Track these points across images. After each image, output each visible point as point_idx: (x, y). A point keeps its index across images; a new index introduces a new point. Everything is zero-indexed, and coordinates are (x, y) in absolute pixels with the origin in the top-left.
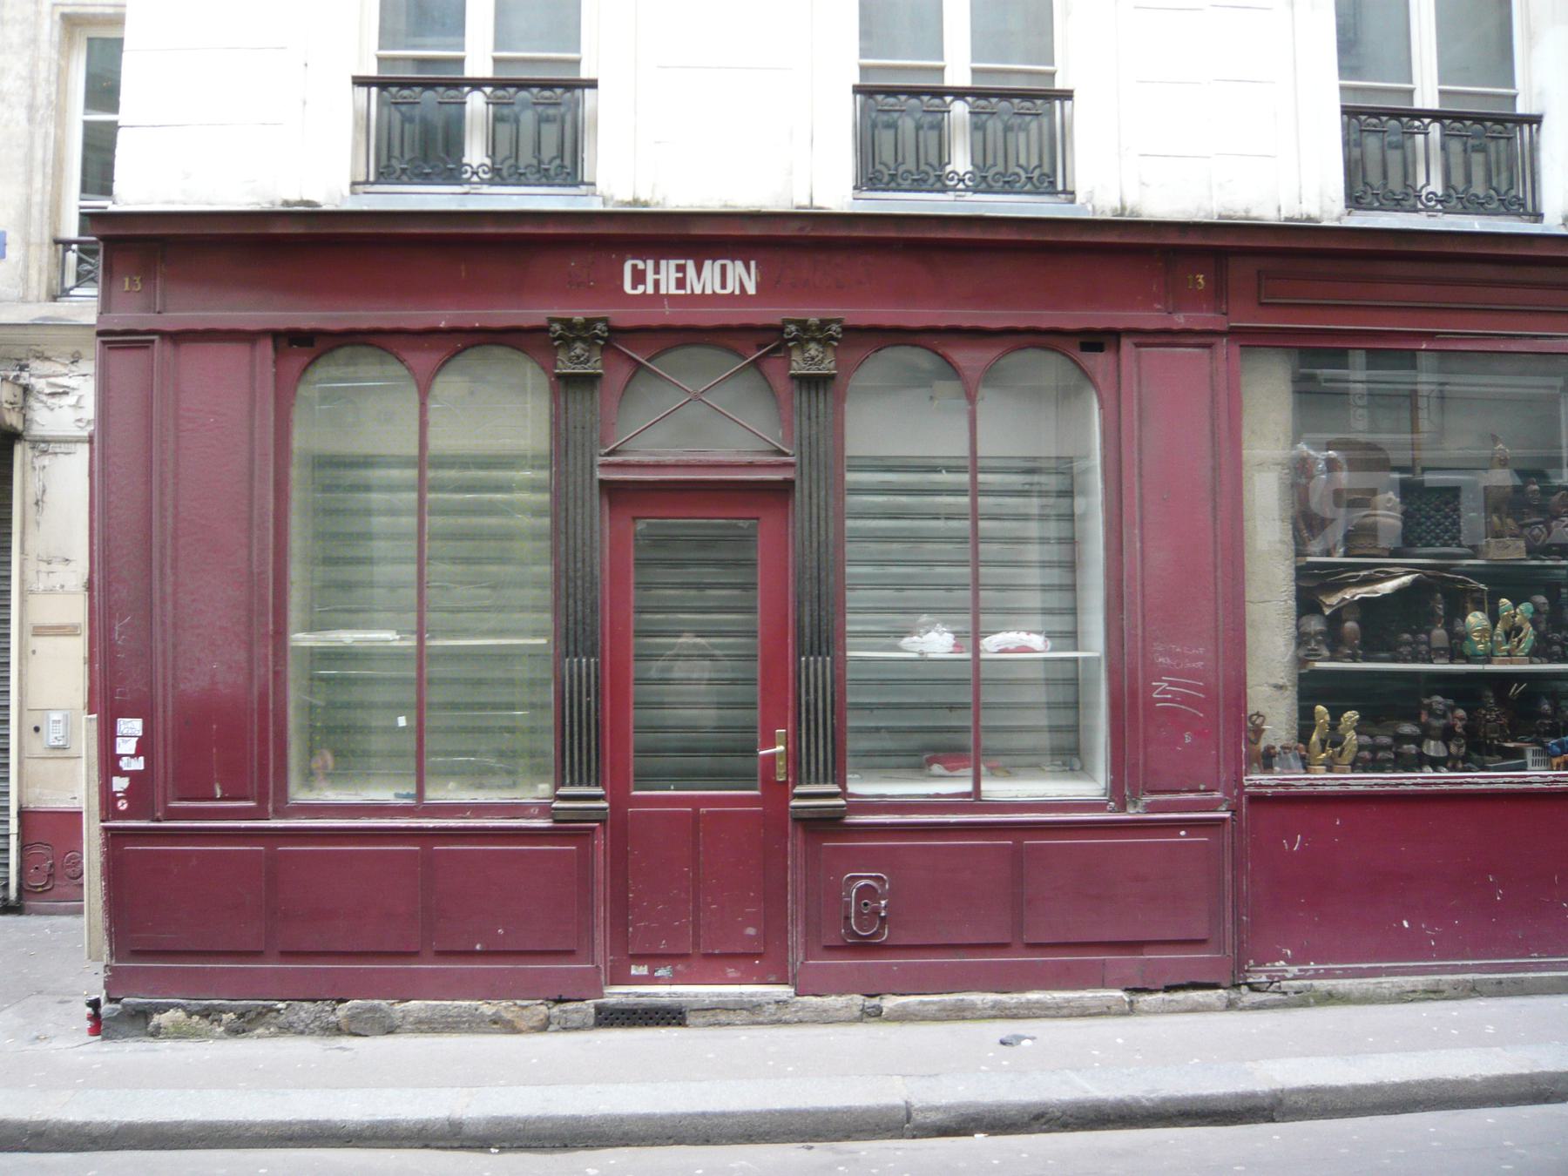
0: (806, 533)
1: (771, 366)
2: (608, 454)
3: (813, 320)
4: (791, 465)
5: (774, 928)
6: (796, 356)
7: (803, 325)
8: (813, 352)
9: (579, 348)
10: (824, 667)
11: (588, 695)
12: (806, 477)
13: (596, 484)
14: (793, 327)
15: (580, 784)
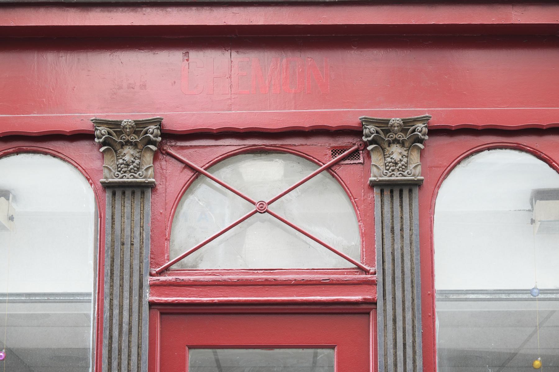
0: (390, 361)
1: (349, 171)
2: (160, 273)
3: (396, 121)
4: (373, 283)
6: (376, 159)
7: (384, 126)
8: (396, 157)
12: (389, 297)
13: (146, 307)
14: (372, 128)
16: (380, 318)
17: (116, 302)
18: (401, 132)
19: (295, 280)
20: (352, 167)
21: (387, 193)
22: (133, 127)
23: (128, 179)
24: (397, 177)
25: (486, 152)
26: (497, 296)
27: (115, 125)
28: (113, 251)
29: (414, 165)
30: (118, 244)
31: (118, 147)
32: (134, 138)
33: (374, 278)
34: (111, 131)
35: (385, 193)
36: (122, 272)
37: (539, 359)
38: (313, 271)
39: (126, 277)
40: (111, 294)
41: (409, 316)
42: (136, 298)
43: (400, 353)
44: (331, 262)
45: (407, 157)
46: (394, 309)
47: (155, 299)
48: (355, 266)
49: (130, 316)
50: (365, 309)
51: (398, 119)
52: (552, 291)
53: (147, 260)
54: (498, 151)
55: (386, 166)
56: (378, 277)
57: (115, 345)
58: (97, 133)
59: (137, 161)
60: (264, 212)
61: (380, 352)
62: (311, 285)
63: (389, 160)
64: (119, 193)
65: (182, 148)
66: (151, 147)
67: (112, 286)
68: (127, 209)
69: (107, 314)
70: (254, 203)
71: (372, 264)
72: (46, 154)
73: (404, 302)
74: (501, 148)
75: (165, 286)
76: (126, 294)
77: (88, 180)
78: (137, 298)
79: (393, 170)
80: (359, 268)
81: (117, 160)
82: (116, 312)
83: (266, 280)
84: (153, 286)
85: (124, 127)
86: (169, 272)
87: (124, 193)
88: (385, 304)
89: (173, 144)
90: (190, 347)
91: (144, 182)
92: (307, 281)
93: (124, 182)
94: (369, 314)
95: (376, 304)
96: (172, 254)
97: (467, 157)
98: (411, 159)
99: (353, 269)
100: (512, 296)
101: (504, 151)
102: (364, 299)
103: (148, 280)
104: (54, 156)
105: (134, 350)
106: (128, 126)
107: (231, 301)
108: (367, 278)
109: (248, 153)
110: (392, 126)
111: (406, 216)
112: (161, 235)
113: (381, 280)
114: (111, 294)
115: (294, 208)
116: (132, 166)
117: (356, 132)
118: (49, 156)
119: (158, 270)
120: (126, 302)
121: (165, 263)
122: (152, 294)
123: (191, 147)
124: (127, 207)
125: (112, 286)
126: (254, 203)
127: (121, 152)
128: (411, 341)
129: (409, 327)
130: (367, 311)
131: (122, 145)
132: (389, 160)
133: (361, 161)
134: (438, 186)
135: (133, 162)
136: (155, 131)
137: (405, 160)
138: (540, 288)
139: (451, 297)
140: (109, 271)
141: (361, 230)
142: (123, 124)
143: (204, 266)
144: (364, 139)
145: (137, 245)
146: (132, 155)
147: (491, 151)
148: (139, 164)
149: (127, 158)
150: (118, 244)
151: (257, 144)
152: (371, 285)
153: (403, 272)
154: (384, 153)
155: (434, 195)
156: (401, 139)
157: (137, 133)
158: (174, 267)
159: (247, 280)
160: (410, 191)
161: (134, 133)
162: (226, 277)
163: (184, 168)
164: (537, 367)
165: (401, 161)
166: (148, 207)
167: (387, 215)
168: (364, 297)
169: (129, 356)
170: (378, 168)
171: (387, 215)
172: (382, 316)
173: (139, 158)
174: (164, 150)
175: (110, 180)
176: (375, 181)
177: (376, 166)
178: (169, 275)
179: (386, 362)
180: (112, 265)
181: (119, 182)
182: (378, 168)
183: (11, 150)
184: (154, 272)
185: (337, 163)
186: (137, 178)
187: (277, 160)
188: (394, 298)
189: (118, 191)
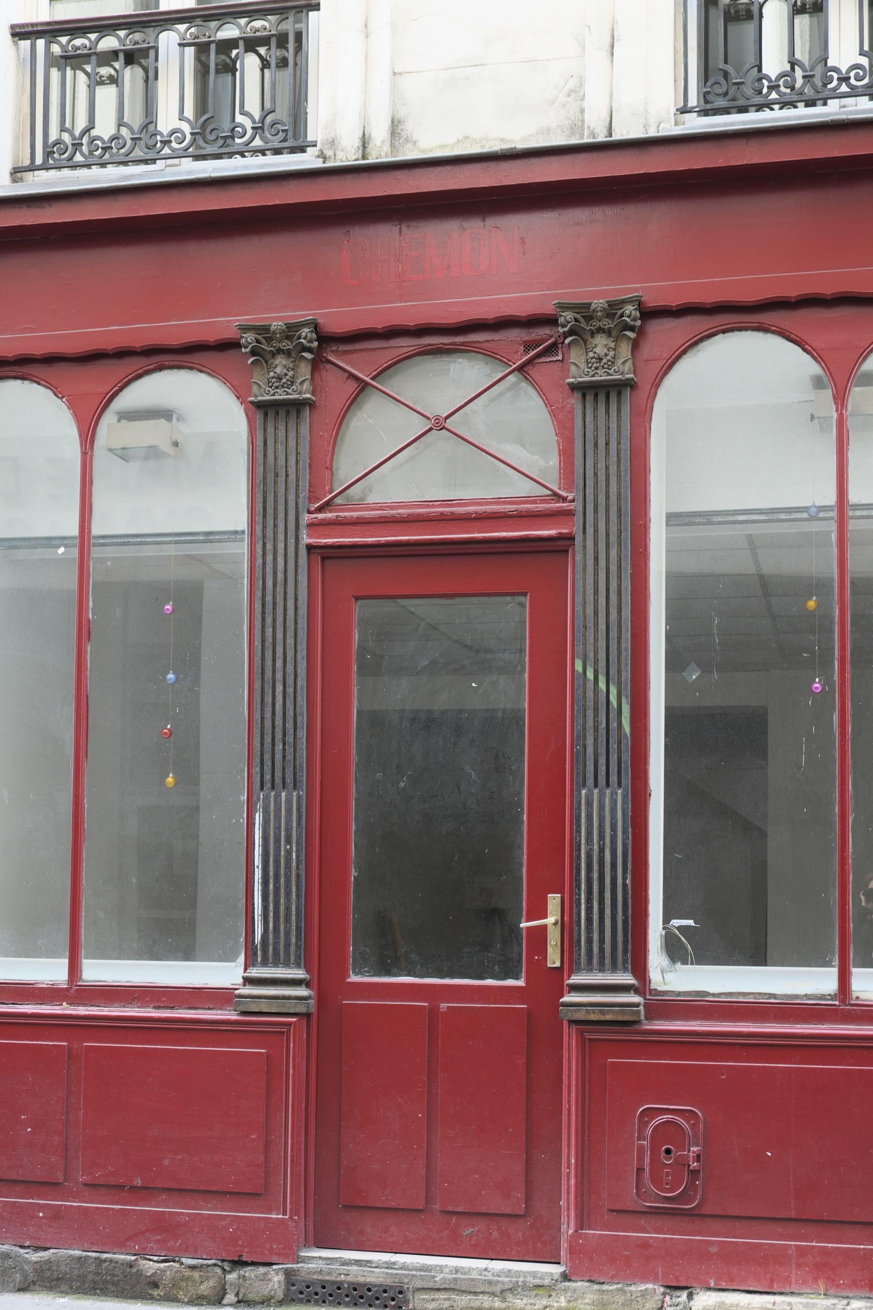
0: (590, 610)
1: (544, 370)
2: (320, 510)
3: (599, 303)
4: (570, 513)
5: (536, 1180)
7: (584, 311)
8: (600, 350)
9: (280, 364)
10: (614, 802)
11: (288, 841)
13: (303, 552)
14: (569, 315)
15: (276, 964)
16: (579, 557)
17: (269, 546)
18: (607, 317)
19: (476, 513)
20: (548, 366)
21: (590, 398)
22: (283, 331)
23: (280, 396)
24: (601, 377)
25: (721, 336)
26: (775, 516)
27: (263, 330)
28: (265, 484)
29: (623, 360)
30: (270, 476)
31: (268, 357)
32: (286, 345)
33: (572, 506)
34: (260, 337)
35: (587, 398)
36: (275, 509)
37: (814, 598)
38: (498, 501)
39: (281, 516)
40: (264, 537)
41: (613, 553)
42: (291, 541)
43: (602, 600)
44: (522, 488)
45: (614, 350)
46: (596, 545)
47: (311, 541)
48: (549, 492)
49: (286, 562)
50: (561, 546)
51: (601, 301)
52: (870, 505)
53: (304, 494)
54: (737, 333)
55: (588, 363)
56: (578, 506)
57: (269, 598)
58: (243, 341)
59: (291, 373)
60: (441, 429)
61: (579, 599)
62: (495, 518)
63: (591, 354)
64: (271, 414)
65: (345, 353)
66: (305, 354)
67: (264, 527)
68: (281, 433)
69: (259, 561)
70: (428, 418)
71: (568, 489)
72: (191, 368)
73: (607, 535)
74: (740, 329)
75: (325, 525)
76: (281, 537)
77: (238, 398)
78: (293, 541)
79: (597, 368)
80: (555, 494)
81: (268, 372)
82: (269, 558)
83: (442, 514)
84: (310, 525)
85: (274, 332)
86: (330, 508)
87: (277, 413)
88: (585, 540)
89: (335, 348)
90: (357, 598)
91: (299, 399)
92: (490, 513)
93: (276, 400)
94: (567, 551)
95: (574, 539)
96: (336, 484)
97: (696, 343)
98: (619, 352)
99: (548, 496)
100: (793, 516)
101: (744, 333)
102: (559, 533)
103: (306, 518)
104: (201, 371)
105: (290, 604)
106: (277, 331)
107: (401, 541)
108: (562, 507)
109: (426, 354)
110: (594, 311)
111: (613, 426)
112: (321, 463)
113: (580, 509)
114: (264, 537)
115: (478, 422)
116: (284, 380)
117: (551, 321)
118: (195, 371)
119: (316, 506)
120: (281, 546)
121: (326, 496)
122: (310, 536)
123: (361, 350)
124: (280, 429)
125: (264, 527)
126: (428, 418)
127: (272, 363)
128: (615, 585)
129: (613, 568)
130: (566, 548)
131: (273, 355)
132: (591, 354)
133: (560, 358)
134: (656, 384)
135: (286, 375)
136: (309, 335)
137: (612, 353)
138: (817, 504)
139: (715, 519)
140: (262, 510)
141: (559, 446)
142: (273, 328)
143: (372, 499)
144: (561, 330)
145: (292, 477)
146: (285, 366)
147: (726, 335)
148: (293, 377)
149: (278, 370)
150: (270, 476)
151: (434, 342)
152: (568, 515)
153: (607, 498)
154: (586, 346)
155: (652, 396)
156: (606, 327)
157: (289, 338)
158: (338, 501)
159: (419, 515)
160: (619, 394)
161: (286, 338)
162: (394, 512)
163: (348, 378)
164: (811, 609)
165: (606, 355)
166: (305, 429)
167: (590, 426)
168: (560, 531)
169: (285, 610)
170: (579, 366)
171: (590, 426)
172: (581, 556)
173: (293, 370)
174: (324, 357)
175: (260, 398)
176: (573, 383)
177: (575, 364)
178: (330, 512)
179: (584, 612)
180: (265, 502)
181: (270, 401)
182: (579, 366)
183: (152, 367)
184: (313, 509)
185: (530, 362)
186: (291, 394)
187: (461, 360)
188: (596, 531)
189: (266, 412)
